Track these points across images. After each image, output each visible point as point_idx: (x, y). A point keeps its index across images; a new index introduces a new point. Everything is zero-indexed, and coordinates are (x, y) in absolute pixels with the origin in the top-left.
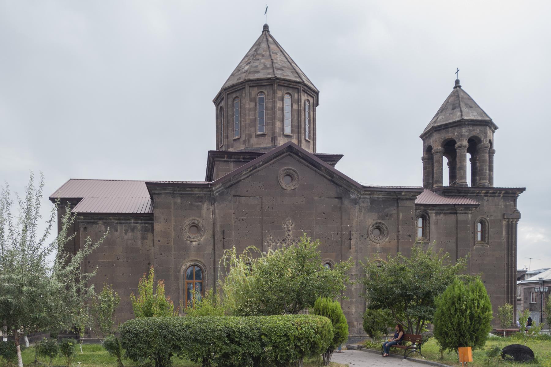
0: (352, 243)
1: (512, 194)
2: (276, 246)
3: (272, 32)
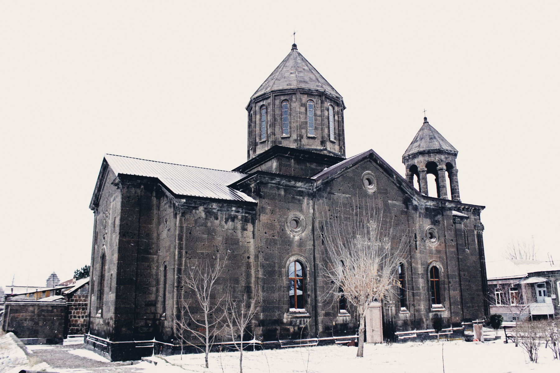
1: (477, 210)
3: (300, 49)
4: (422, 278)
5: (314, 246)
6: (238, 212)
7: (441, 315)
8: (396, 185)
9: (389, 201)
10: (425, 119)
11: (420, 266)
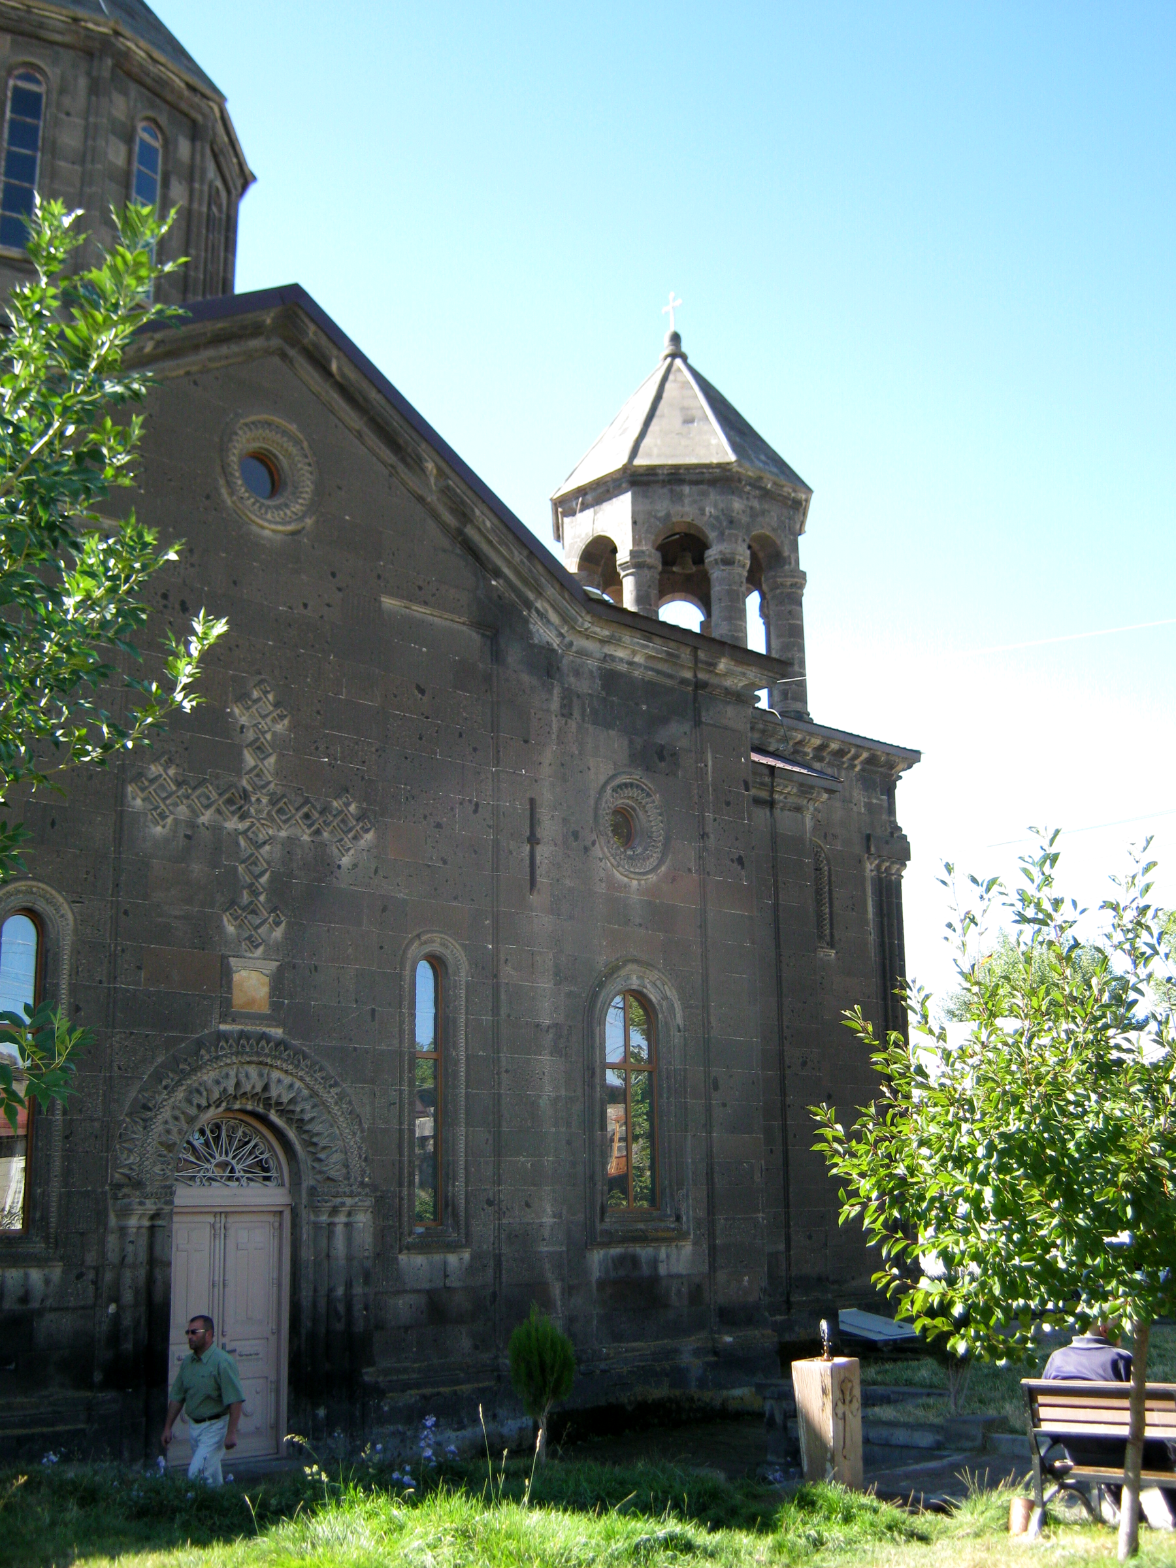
0: (538, 858)
1: (881, 766)
2: (192, 825)
4: (556, 1051)
7: (655, 1262)
8: (436, 516)
9: (388, 602)
10: (676, 338)
11: (545, 984)
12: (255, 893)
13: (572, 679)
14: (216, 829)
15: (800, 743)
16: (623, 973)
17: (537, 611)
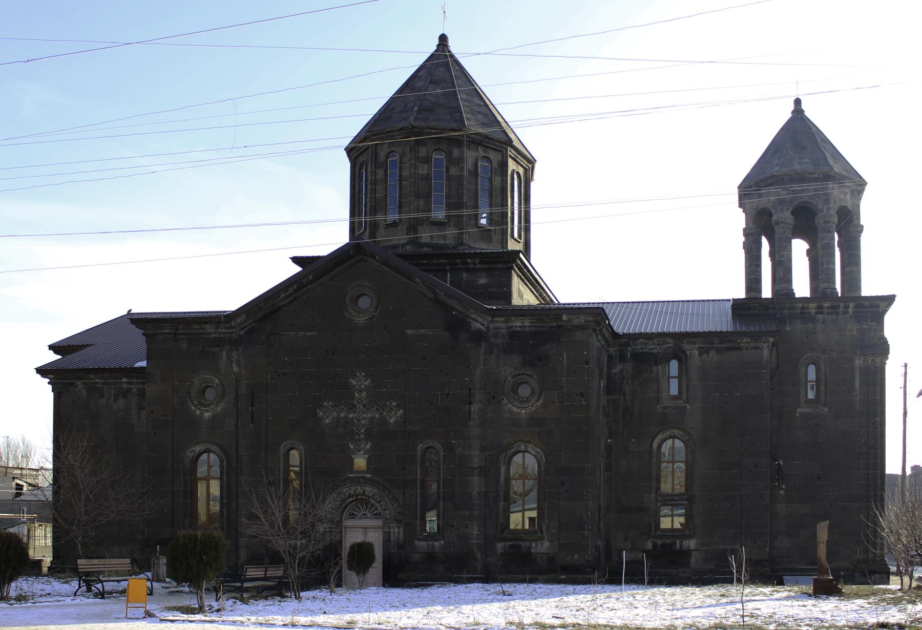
0: (472, 410)
2: (338, 418)
5: (237, 425)
6: (131, 383)
7: (530, 548)
12: (359, 435)
13: (493, 339)
14: (346, 417)
15: (803, 308)
16: (516, 445)
17: (473, 319)
